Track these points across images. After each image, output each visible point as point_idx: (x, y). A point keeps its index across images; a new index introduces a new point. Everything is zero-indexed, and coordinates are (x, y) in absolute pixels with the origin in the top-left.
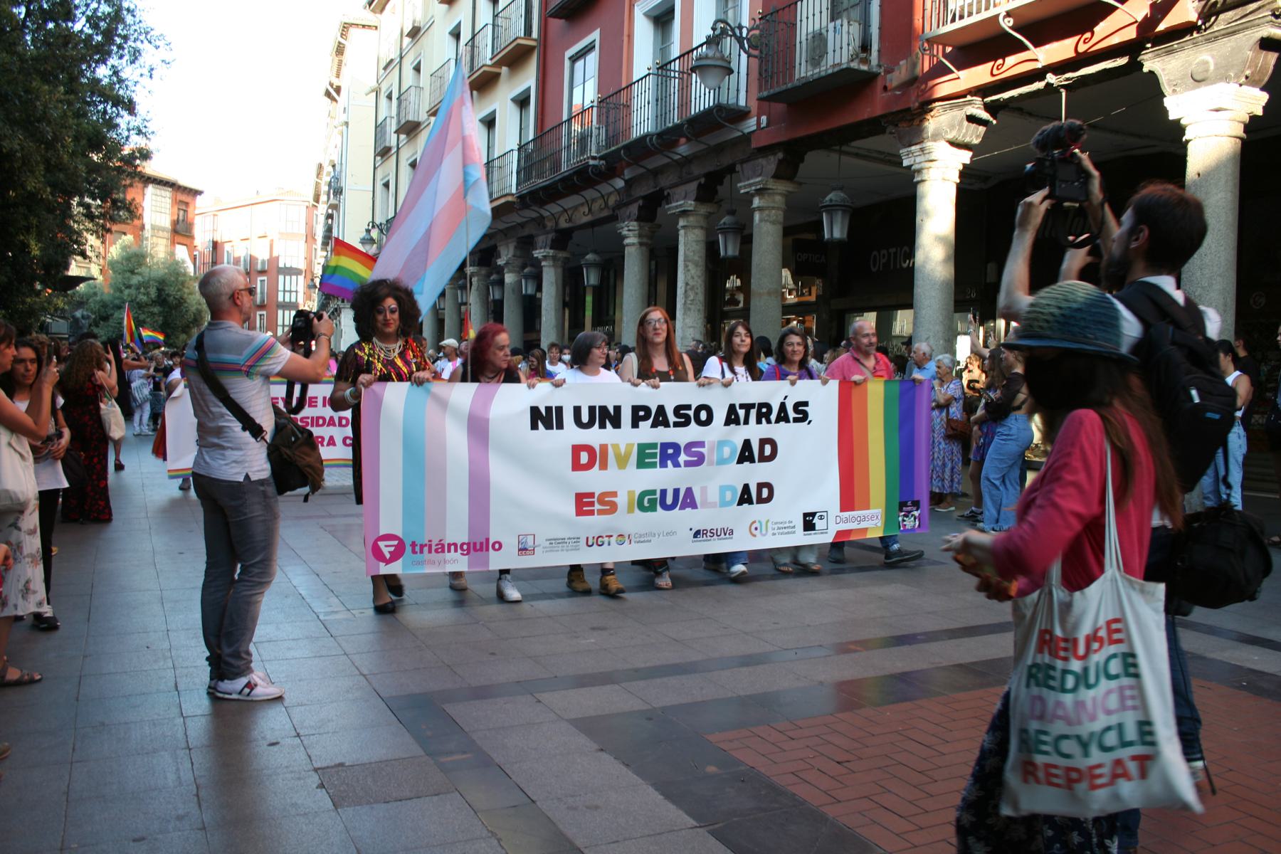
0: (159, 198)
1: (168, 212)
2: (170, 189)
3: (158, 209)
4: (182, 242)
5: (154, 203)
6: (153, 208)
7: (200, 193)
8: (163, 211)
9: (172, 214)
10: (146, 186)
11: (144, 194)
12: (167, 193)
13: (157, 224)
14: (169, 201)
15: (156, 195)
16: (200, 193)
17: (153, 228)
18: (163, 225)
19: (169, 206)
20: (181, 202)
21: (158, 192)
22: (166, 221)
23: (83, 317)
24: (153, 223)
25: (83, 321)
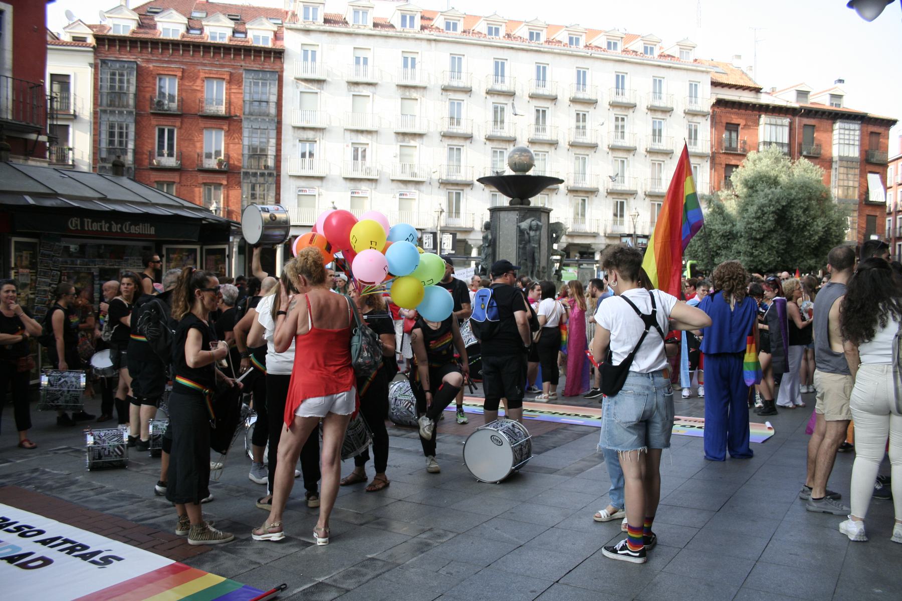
0: (847, 132)
1: (857, 143)
2: (860, 122)
3: (847, 142)
4: (874, 170)
5: (842, 136)
6: (842, 141)
7: (893, 122)
8: (852, 142)
9: (861, 145)
10: (834, 123)
11: (832, 131)
12: (856, 126)
13: (846, 155)
14: (857, 133)
15: (845, 129)
16: (893, 122)
17: (841, 159)
18: (851, 155)
19: (857, 138)
20: (872, 133)
21: (847, 126)
22: (854, 152)
23: (531, 228)
24: (842, 154)
25: (532, 233)
